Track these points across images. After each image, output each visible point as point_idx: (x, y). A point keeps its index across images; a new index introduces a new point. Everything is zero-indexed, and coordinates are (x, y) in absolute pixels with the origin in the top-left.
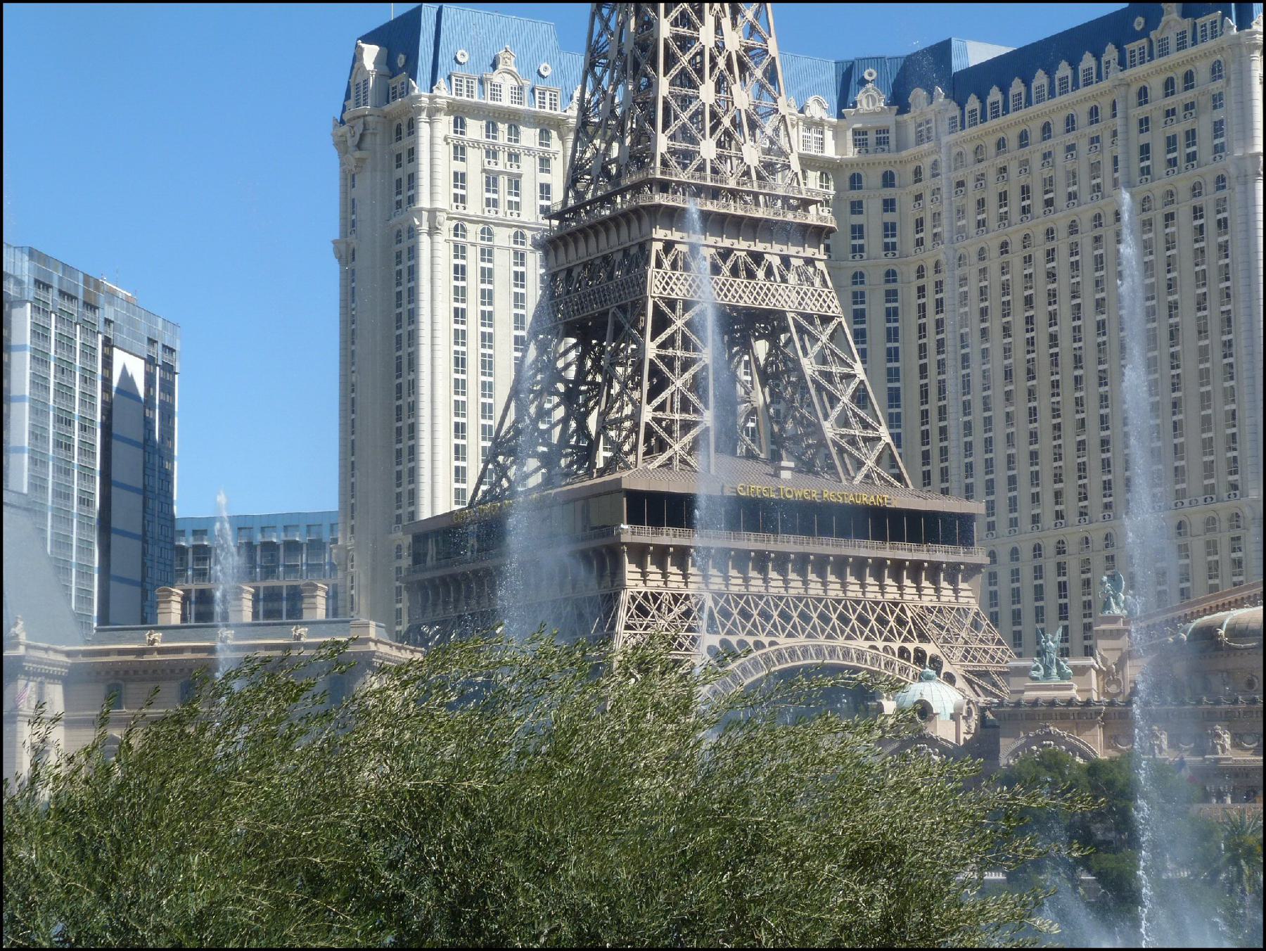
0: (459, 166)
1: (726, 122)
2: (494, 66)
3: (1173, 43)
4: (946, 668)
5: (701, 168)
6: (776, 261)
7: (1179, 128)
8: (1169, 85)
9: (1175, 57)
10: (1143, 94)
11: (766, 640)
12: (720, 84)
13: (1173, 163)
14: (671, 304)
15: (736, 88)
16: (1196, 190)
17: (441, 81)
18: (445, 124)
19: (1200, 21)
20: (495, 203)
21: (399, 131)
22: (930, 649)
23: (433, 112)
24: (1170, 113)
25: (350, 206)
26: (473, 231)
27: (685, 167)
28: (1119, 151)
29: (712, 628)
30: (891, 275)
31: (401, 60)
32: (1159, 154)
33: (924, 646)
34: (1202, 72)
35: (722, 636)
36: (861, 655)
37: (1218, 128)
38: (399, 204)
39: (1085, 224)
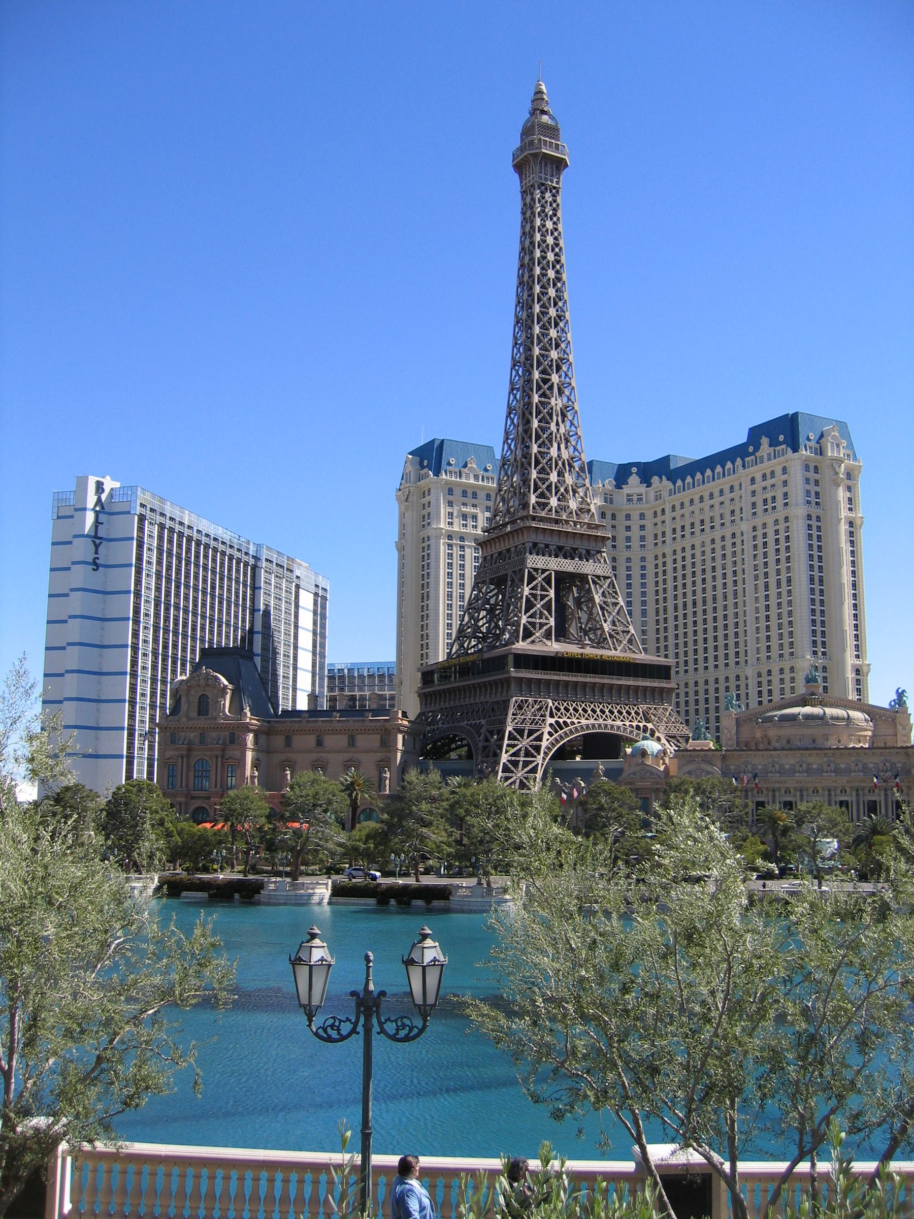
0: (449, 510)
1: (562, 490)
2: (465, 466)
3: (765, 458)
4: (657, 734)
5: (550, 510)
6: (584, 552)
7: (769, 496)
8: (764, 476)
9: (766, 464)
10: (753, 480)
11: (576, 721)
13: (766, 510)
14: (536, 570)
15: (567, 475)
19: (777, 448)
20: (466, 525)
21: (424, 493)
22: (650, 726)
24: (764, 488)
25: (402, 526)
27: (544, 509)
28: (743, 505)
29: (552, 716)
30: (629, 560)
32: (760, 507)
33: (648, 725)
35: (556, 719)
36: (619, 728)
37: (786, 495)
38: (424, 526)
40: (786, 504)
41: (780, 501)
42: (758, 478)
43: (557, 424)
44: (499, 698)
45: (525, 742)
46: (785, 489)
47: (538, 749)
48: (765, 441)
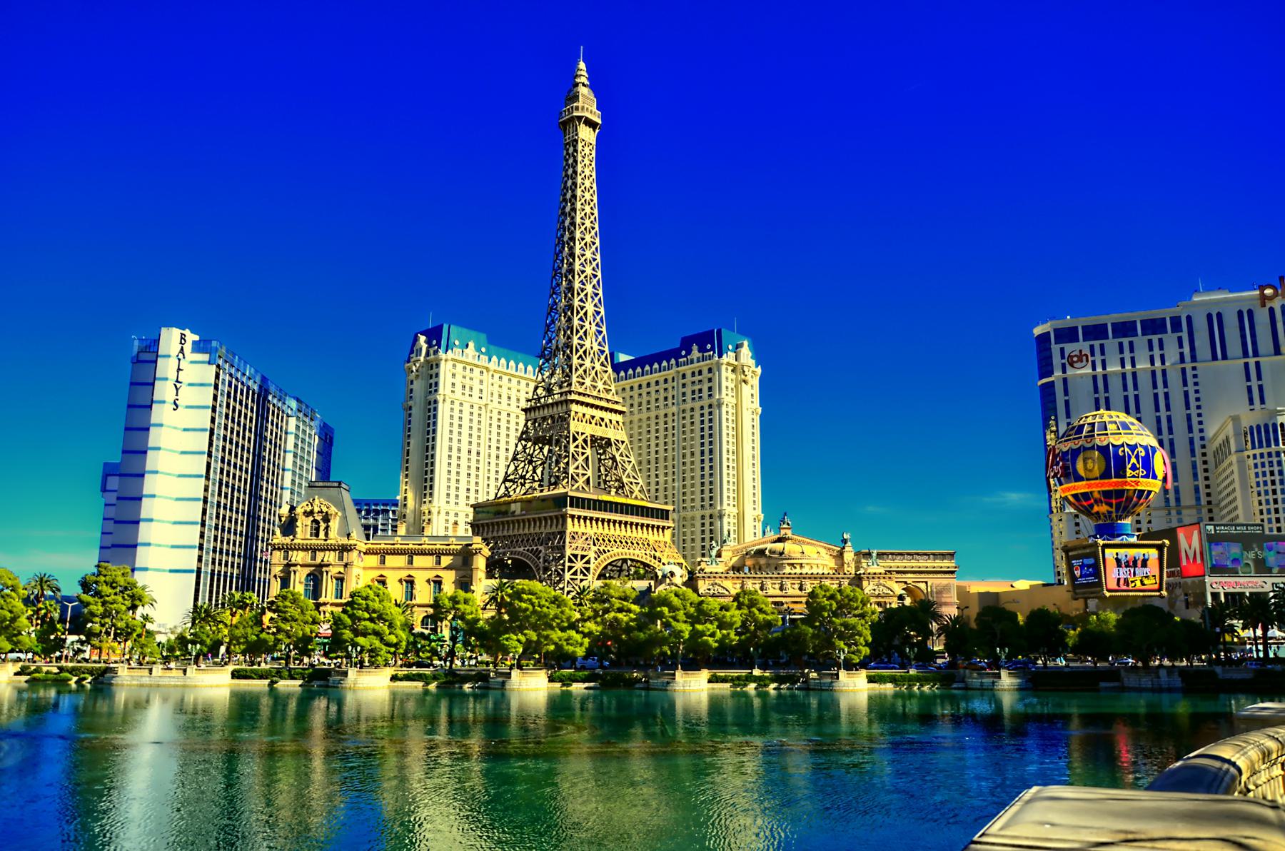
3: (695, 360)
7: (697, 387)
8: (693, 374)
9: (696, 365)
10: (684, 376)
11: (610, 549)
12: (592, 361)
13: (693, 399)
16: (702, 408)
17: (450, 351)
18: (450, 364)
21: (432, 366)
23: (446, 360)
24: (693, 383)
26: (457, 403)
28: (675, 393)
31: (434, 342)
32: (689, 397)
34: (705, 371)
39: (662, 416)
40: (710, 396)
41: (705, 393)
42: (689, 374)
43: (590, 323)
44: (554, 529)
45: (579, 565)
46: (710, 384)
47: (588, 569)
48: (695, 347)
